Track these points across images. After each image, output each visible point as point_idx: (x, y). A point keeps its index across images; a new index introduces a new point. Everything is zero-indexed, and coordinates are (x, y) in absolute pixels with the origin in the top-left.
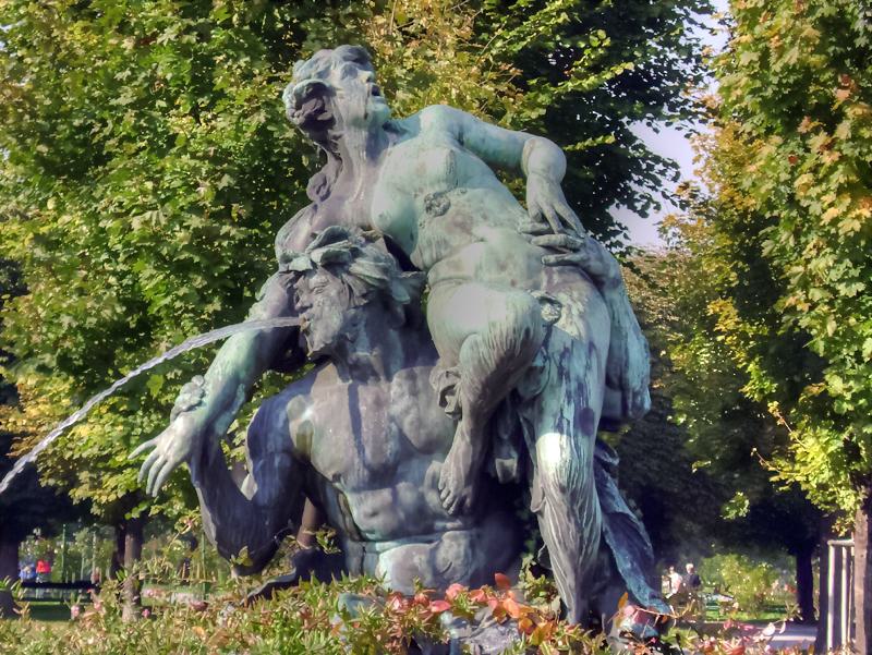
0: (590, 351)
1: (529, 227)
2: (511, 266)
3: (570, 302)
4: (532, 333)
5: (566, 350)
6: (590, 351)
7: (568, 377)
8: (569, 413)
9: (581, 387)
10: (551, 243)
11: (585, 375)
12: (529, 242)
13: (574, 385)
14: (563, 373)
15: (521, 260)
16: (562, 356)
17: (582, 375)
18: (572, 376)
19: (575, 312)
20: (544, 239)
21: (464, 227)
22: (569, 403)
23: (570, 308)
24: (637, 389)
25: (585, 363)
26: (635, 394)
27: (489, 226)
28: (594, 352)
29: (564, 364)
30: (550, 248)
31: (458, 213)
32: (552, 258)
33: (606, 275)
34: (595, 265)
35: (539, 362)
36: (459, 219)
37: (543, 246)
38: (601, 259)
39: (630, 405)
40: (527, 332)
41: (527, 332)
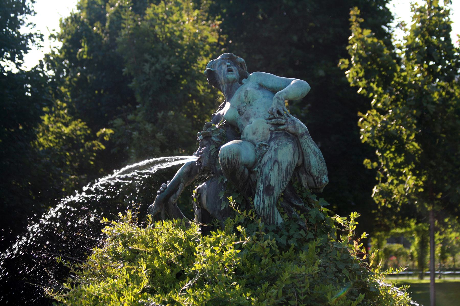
0: (274, 163)
1: (267, 117)
2: (257, 133)
3: (273, 145)
4: (230, 159)
5: (264, 163)
6: (274, 163)
7: (263, 174)
8: (261, 188)
9: (267, 177)
10: (273, 123)
11: (269, 173)
12: (267, 123)
13: (264, 177)
14: (262, 173)
15: (260, 130)
16: (263, 166)
17: (267, 173)
18: (264, 173)
19: (273, 148)
20: (271, 121)
21: (247, 119)
22: (262, 184)
23: (272, 146)
24: (317, 175)
25: (270, 168)
26: (317, 178)
27: (255, 118)
28: (276, 164)
29: (263, 169)
30: (273, 124)
31: (247, 114)
32: (273, 129)
33: (298, 133)
34: (291, 128)
35: (256, 169)
36: (246, 116)
37: (271, 124)
38: (295, 127)
39: (316, 182)
40: (228, 159)
41: (228, 159)
